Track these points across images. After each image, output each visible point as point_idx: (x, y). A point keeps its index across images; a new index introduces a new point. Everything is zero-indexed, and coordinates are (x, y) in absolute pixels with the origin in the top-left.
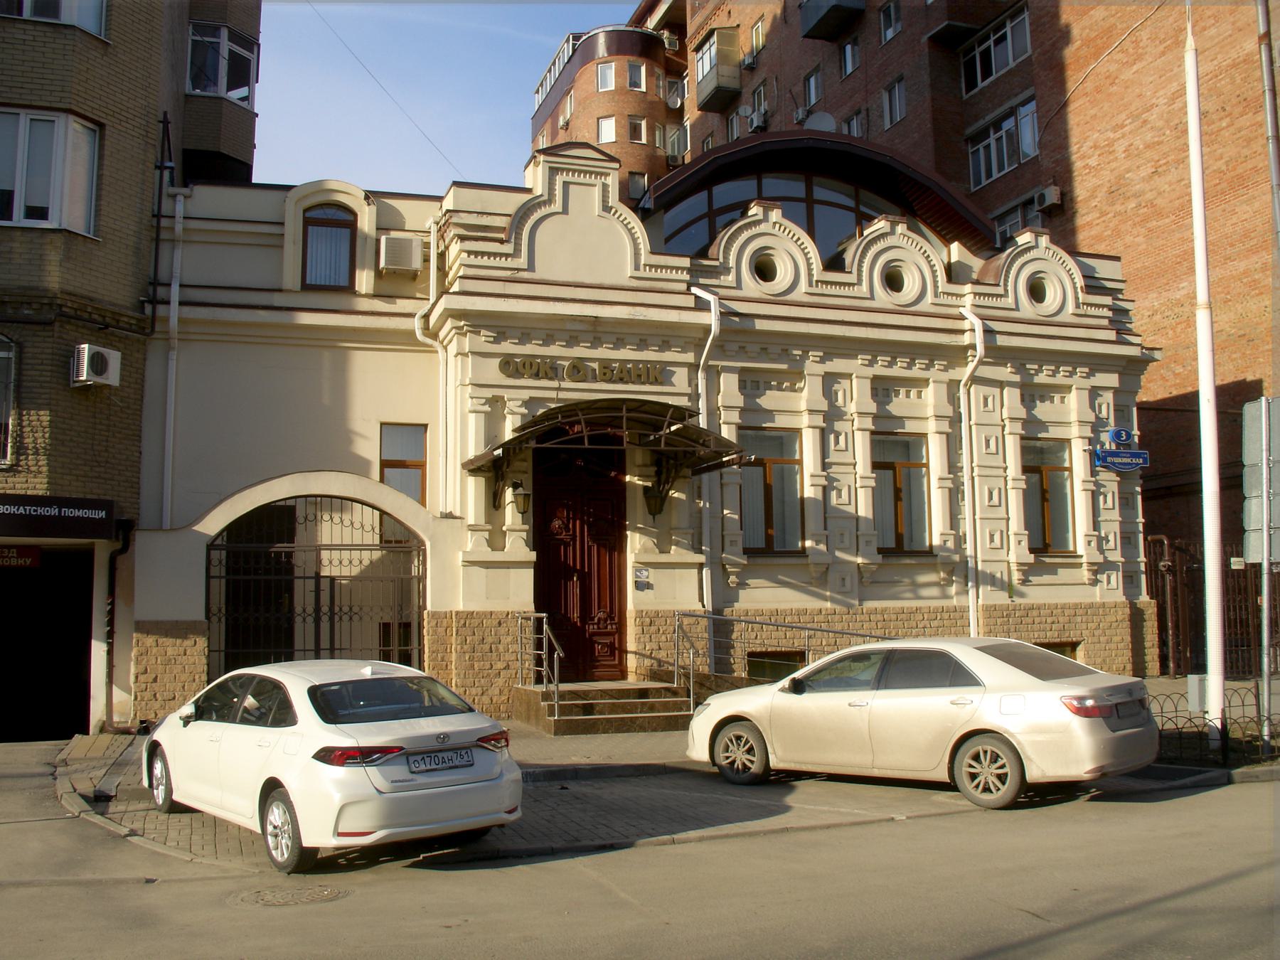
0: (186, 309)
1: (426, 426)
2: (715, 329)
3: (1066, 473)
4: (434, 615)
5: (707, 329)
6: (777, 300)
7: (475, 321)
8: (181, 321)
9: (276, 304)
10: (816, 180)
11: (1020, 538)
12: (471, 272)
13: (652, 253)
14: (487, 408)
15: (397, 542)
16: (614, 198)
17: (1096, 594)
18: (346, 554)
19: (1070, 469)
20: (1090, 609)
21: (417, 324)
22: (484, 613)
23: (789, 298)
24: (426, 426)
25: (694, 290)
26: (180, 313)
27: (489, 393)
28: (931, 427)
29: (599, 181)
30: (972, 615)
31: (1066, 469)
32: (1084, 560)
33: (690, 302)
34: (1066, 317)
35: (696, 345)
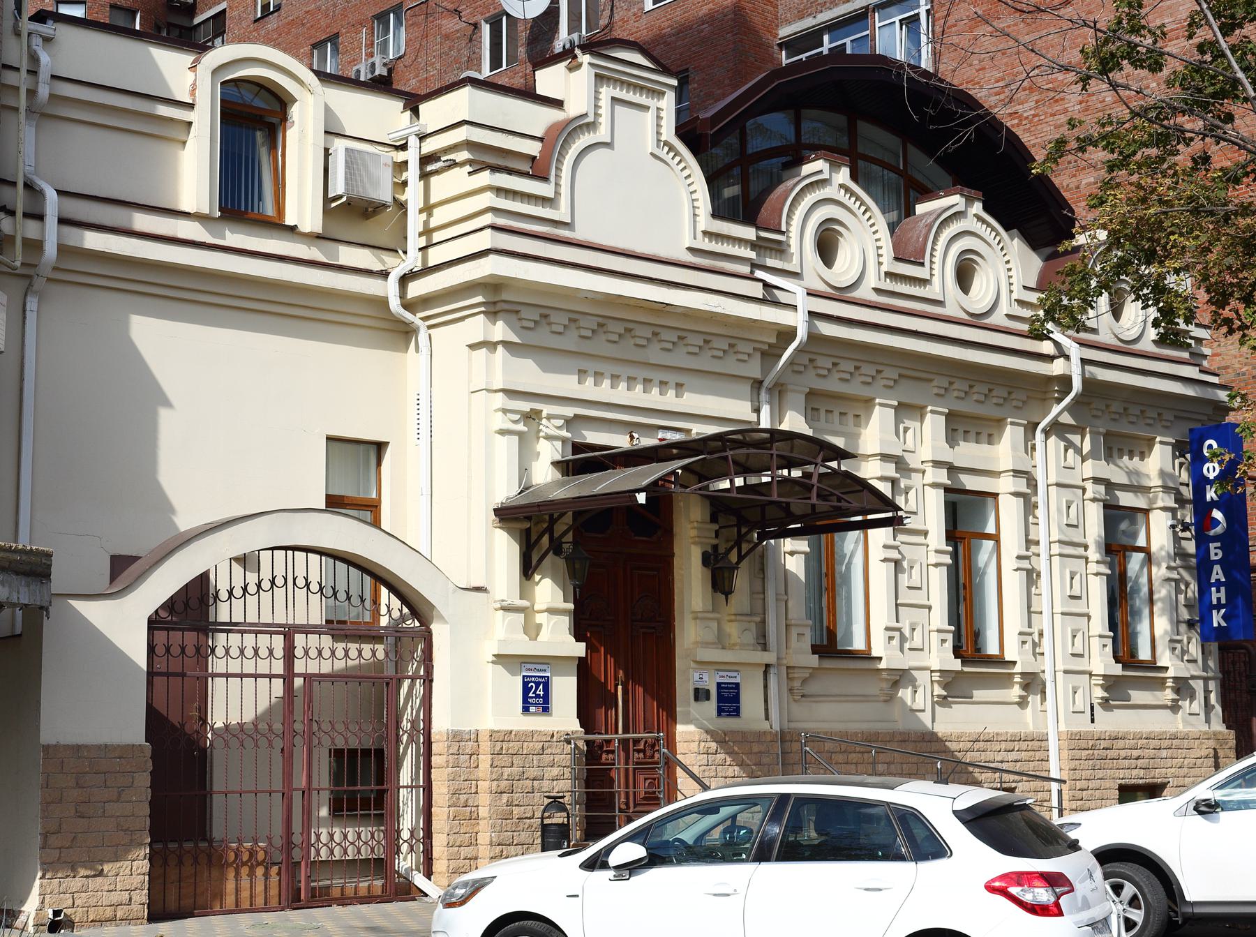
0: (67, 230)
1: (380, 447)
2: (802, 334)
3: (988, 545)
4: (456, 737)
5: (787, 334)
6: (976, 320)
7: (497, 298)
8: (63, 250)
9: (181, 235)
10: (806, 113)
11: (944, 636)
12: (502, 221)
13: (896, 259)
14: (521, 427)
15: (339, 622)
16: (668, 132)
17: (1177, 723)
18: (249, 639)
19: (996, 538)
20: (1175, 740)
21: (390, 289)
22: (525, 733)
23: (987, 321)
24: (380, 447)
25: (759, 274)
26: (43, 231)
27: (526, 406)
28: (1005, 485)
29: (651, 102)
30: (1053, 745)
31: (988, 537)
32: (1018, 669)
33: (757, 290)
34: (998, 319)
35: (764, 354)
